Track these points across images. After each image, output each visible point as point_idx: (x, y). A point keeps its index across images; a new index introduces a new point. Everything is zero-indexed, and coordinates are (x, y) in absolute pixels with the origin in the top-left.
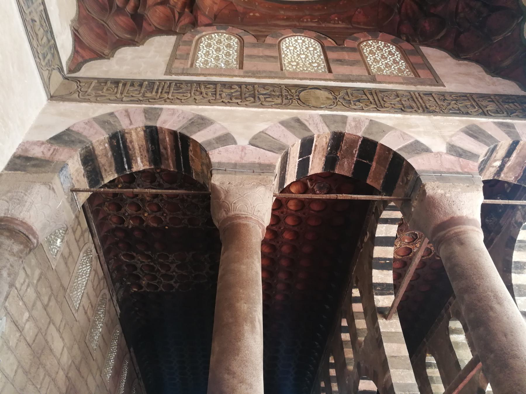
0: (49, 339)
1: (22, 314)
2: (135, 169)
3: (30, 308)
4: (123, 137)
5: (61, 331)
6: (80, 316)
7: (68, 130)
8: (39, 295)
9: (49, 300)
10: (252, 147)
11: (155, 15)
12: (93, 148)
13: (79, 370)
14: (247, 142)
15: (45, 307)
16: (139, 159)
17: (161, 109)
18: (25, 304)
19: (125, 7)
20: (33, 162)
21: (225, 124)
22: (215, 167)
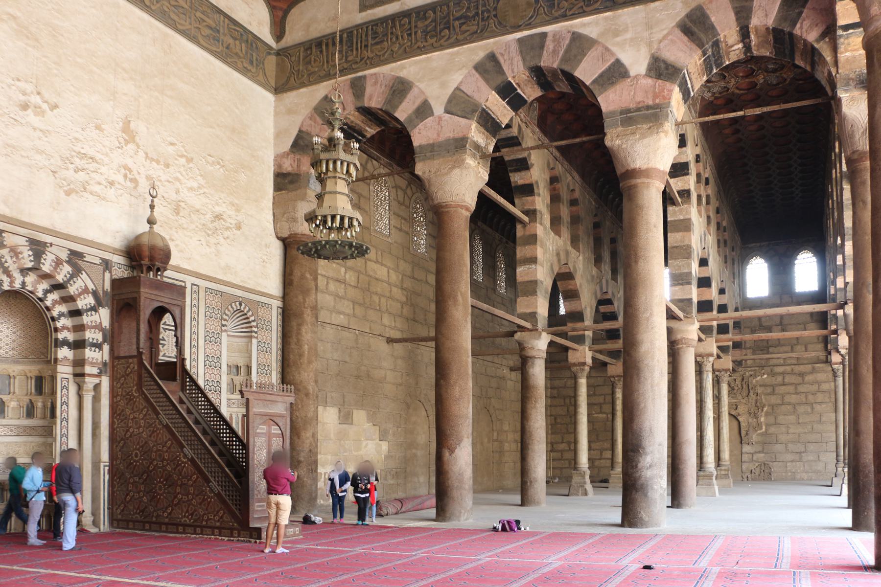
0: (371, 273)
1: (339, 271)
2: (369, 136)
6: (397, 237)
7: (300, 131)
13: (414, 278)
14: (443, 110)
16: (367, 128)
17: (365, 77)
20: (290, 178)
21: (422, 86)
22: (417, 150)
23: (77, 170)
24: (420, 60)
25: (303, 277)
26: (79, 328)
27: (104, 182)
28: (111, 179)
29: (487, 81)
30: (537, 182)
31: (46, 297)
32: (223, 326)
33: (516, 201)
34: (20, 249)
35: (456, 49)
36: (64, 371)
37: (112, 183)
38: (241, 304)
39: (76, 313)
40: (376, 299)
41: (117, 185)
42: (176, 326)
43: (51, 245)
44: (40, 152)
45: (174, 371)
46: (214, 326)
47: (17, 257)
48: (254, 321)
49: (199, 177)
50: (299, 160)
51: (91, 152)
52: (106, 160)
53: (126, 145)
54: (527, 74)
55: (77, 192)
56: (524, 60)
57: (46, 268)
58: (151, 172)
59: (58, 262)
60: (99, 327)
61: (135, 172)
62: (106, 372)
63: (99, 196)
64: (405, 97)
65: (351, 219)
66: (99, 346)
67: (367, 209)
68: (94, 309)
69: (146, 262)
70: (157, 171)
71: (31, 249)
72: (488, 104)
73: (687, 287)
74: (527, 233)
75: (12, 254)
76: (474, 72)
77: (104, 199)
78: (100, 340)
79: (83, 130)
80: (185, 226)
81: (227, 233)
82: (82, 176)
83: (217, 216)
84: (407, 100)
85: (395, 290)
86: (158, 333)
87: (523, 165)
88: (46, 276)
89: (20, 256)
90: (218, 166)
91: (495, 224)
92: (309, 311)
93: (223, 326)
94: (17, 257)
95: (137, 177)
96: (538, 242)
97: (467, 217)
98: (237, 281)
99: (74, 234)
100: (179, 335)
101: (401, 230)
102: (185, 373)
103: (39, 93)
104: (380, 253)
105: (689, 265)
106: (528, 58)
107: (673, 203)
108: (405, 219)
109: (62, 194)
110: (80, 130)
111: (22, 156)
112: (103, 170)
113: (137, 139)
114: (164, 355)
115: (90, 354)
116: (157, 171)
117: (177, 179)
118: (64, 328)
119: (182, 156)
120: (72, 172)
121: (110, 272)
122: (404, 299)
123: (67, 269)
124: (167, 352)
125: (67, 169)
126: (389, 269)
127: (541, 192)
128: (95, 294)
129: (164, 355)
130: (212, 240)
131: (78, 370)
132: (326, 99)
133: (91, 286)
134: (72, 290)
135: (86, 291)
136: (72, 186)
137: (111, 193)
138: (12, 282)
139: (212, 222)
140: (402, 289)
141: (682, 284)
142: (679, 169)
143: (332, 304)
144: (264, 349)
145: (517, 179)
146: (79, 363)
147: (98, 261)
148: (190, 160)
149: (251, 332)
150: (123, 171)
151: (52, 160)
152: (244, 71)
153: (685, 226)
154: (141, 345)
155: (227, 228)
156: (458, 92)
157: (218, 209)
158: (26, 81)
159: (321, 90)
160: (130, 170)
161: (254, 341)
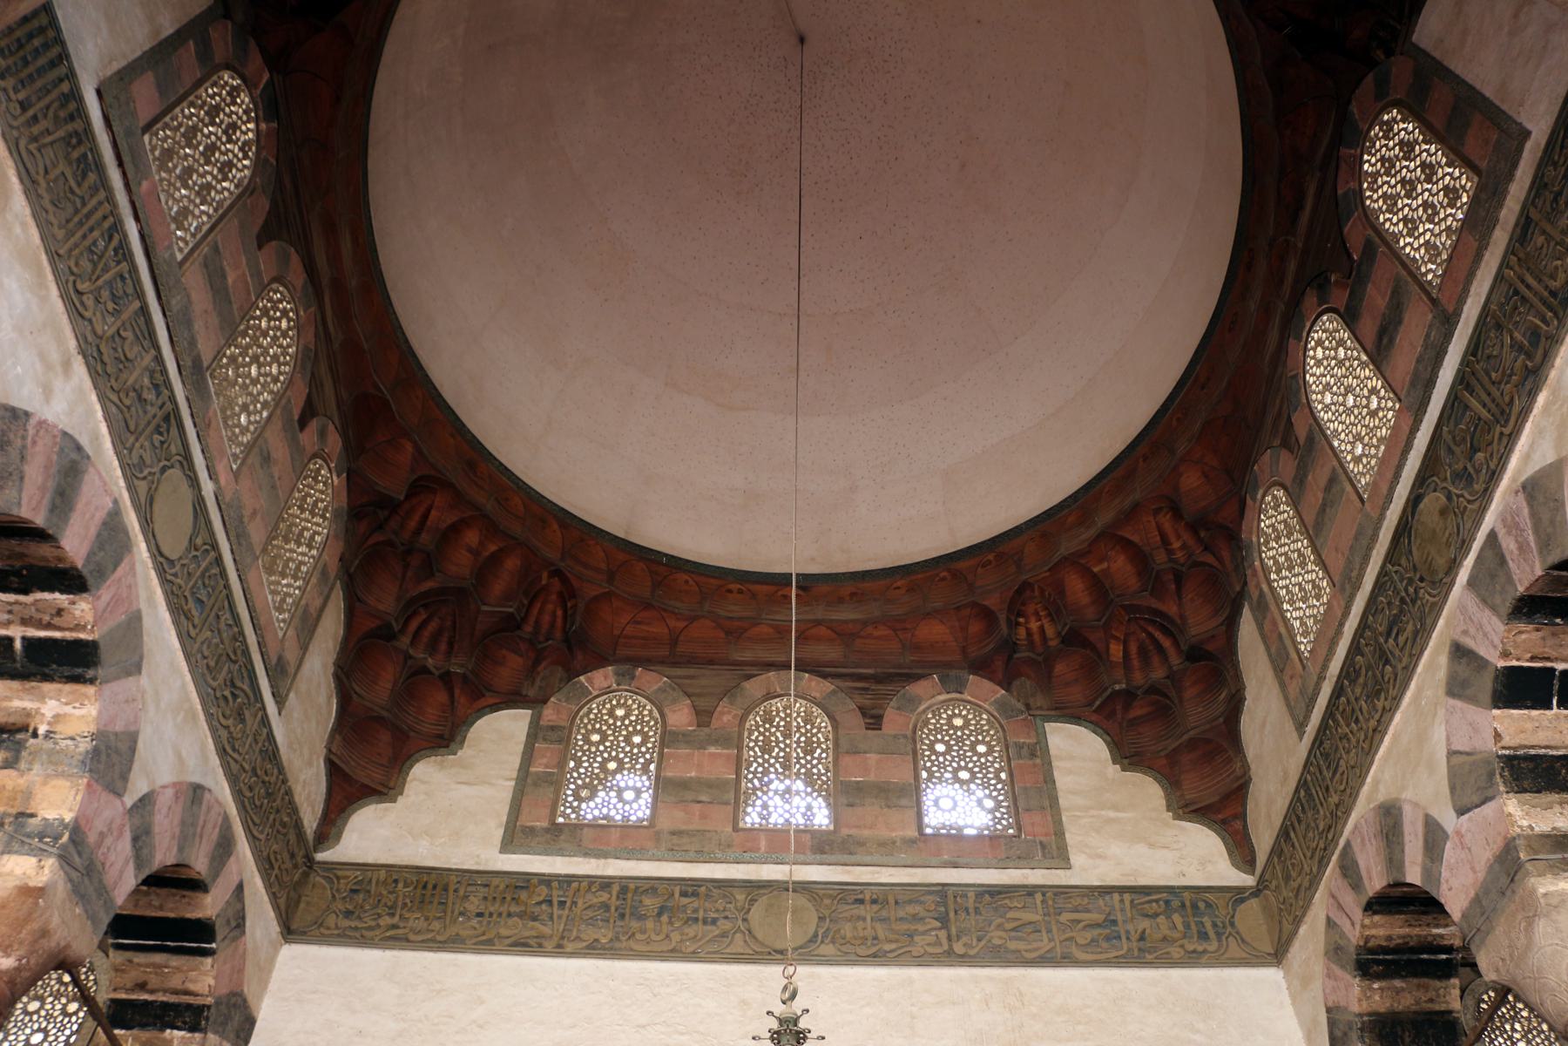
11: (1199, 622)
19: (1170, 667)
24: (1389, 750)
29: (1473, 700)
35: (1413, 685)
54: (1522, 626)
56: (1493, 609)
64: (1402, 834)
72: (1507, 741)
76: (1452, 702)
84: (1407, 838)
106: (1498, 600)
156: (1456, 760)
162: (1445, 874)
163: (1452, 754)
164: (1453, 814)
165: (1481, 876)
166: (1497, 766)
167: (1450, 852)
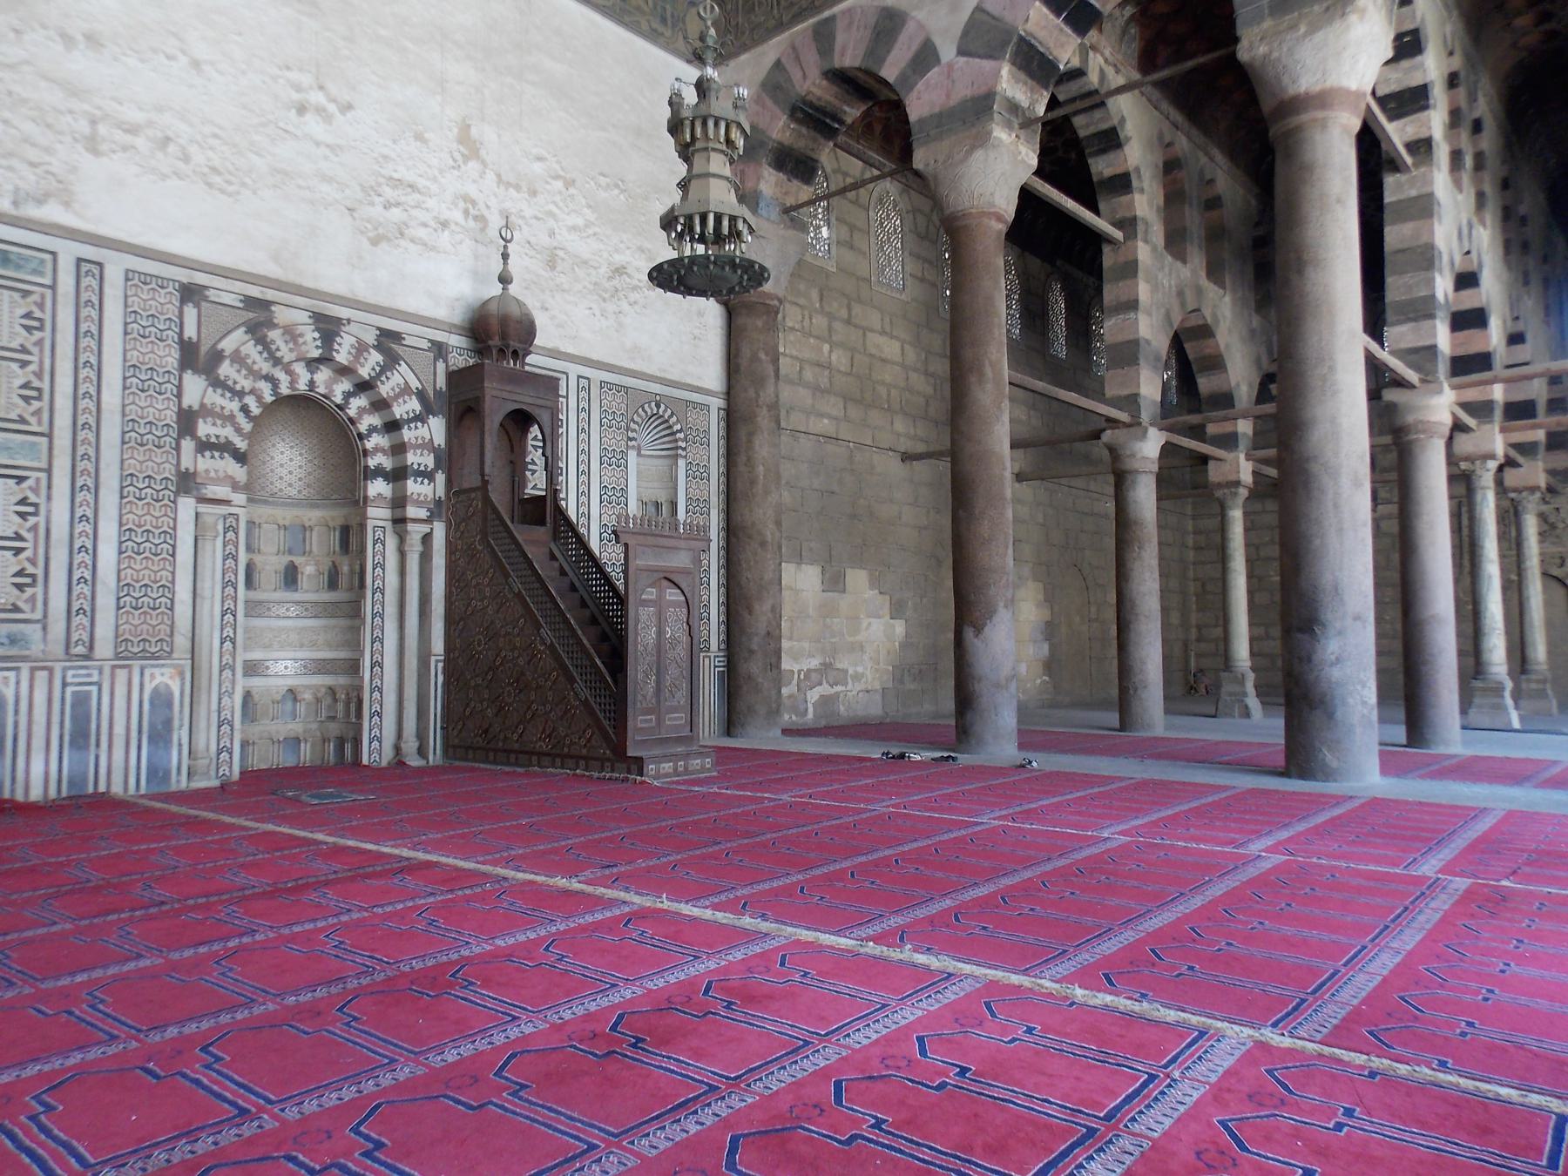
0: (873, 351)
1: (821, 350)
2: (849, 120)
3: (828, 337)
4: (804, 102)
5: (888, 329)
8: (831, 317)
9: (849, 309)
10: (963, 60)
12: (780, 143)
15: (848, 322)
16: (846, 108)
18: (817, 338)
23: (388, 206)
25: (754, 358)
26: (399, 449)
27: (432, 223)
28: (443, 217)
30: (1137, 170)
31: (347, 403)
32: (631, 439)
33: (1102, 206)
34: (301, 329)
36: (378, 515)
37: (444, 224)
38: (658, 406)
39: (393, 426)
40: (883, 391)
41: (453, 227)
42: (544, 440)
43: (349, 321)
44: (328, 179)
45: (544, 511)
46: (616, 441)
47: (296, 343)
48: (680, 431)
49: (586, 210)
50: (742, 172)
51: (409, 176)
52: (434, 188)
53: (465, 163)
55: (389, 240)
57: (342, 357)
58: (507, 205)
59: (361, 349)
60: (429, 446)
61: (482, 206)
62: (440, 516)
63: (425, 245)
65: (733, 219)
66: (428, 475)
67: (865, 248)
68: (420, 418)
69: (495, 342)
70: (517, 203)
71: (317, 329)
73: (1426, 324)
74: (1121, 259)
75: (288, 337)
77: (433, 248)
78: (431, 465)
79: (394, 142)
80: (566, 286)
81: (634, 296)
82: (396, 214)
83: (617, 270)
85: (914, 376)
86: (524, 453)
87: (1111, 140)
88: (344, 371)
89: (301, 340)
90: (616, 192)
91: (1059, 250)
92: (765, 410)
93: (631, 439)
94: (296, 343)
95: (486, 213)
96: (1140, 274)
97: (1000, 232)
98: (651, 370)
99: (386, 304)
100: (549, 453)
101: (922, 280)
102: (560, 513)
103: (321, 88)
104: (887, 320)
105: (1431, 283)
107: (1395, 166)
108: (930, 263)
109: (366, 244)
110: (389, 143)
111: (299, 187)
112: (431, 203)
113: (483, 153)
114: (534, 487)
115: (413, 487)
116: (517, 203)
117: (550, 214)
118: (377, 449)
119: (557, 177)
120: (380, 208)
121: (446, 361)
122: (929, 390)
123: (375, 357)
124: (536, 483)
125: (372, 204)
126: (903, 342)
127: (1146, 185)
128: (421, 395)
129: (534, 487)
130: (611, 307)
131: (398, 514)
132: (778, 64)
133: (415, 384)
134: (385, 389)
135: (406, 390)
136: (381, 231)
137: (445, 238)
138: (293, 383)
139: (610, 278)
140: (926, 373)
141: (1415, 320)
142: (1409, 101)
143: (809, 401)
144: (697, 474)
145: (1102, 167)
146: (399, 502)
147: (425, 345)
148: (569, 183)
149: (677, 448)
150: (462, 204)
151: (347, 191)
152: (653, 36)
153: (1424, 207)
154: (487, 470)
155: (635, 288)
157: (619, 259)
158: (301, 70)
159: (772, 50)
160: (474, 203)
161: (681, 463)
162: (920, 85)
163: (979, 9)
164: (954, 51)
165: (952, 103)
166: (1015, 39)
167: (934, 74)
